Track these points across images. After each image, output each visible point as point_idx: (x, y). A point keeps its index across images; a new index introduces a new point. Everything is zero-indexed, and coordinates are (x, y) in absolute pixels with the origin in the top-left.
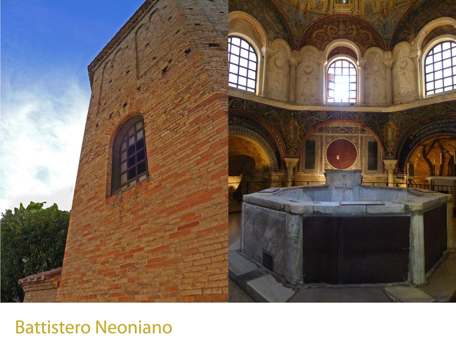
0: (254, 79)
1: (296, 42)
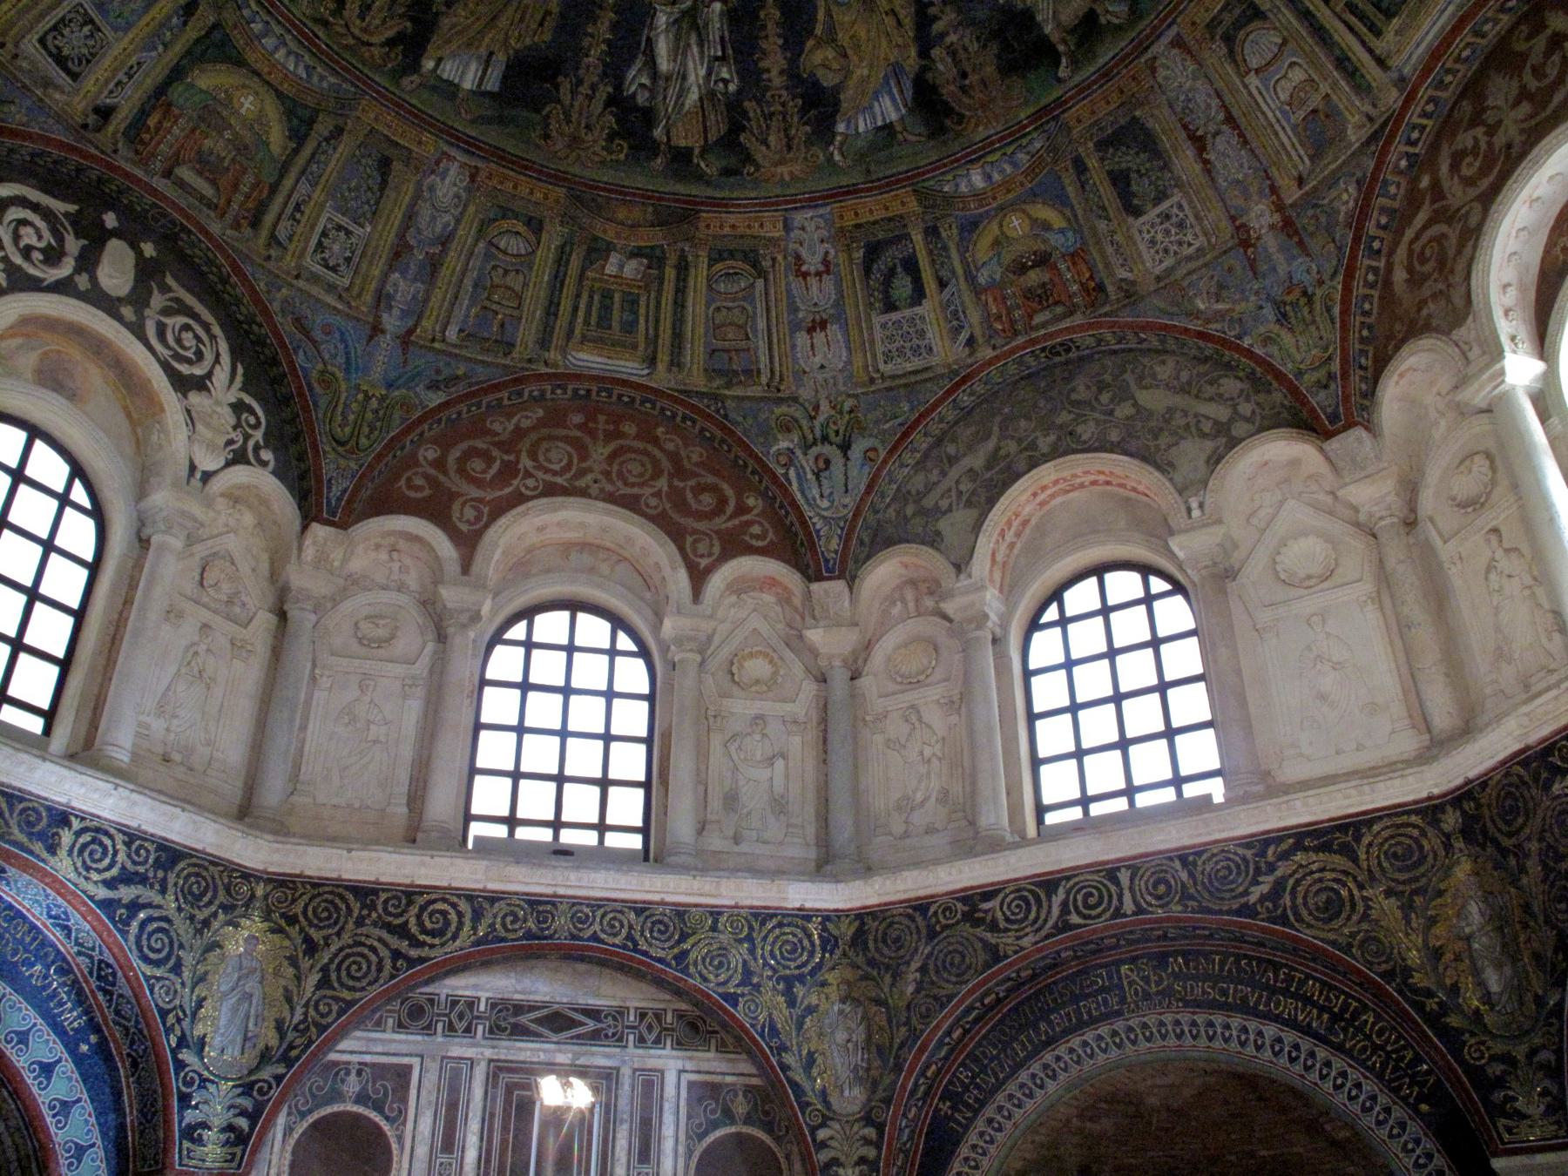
1: (1322, 394)
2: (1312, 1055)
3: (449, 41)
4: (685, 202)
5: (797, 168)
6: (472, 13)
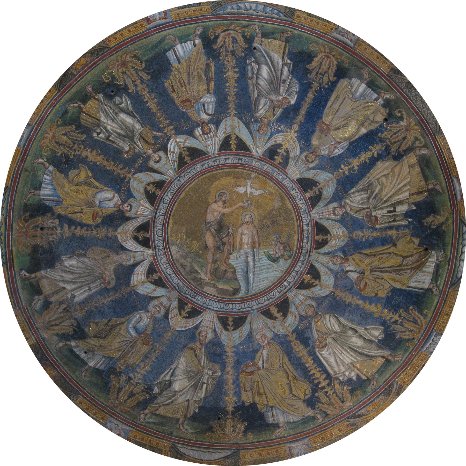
3: (197, 53)
4: (67, 88)
5: (47, 141)
6: (197, 69)
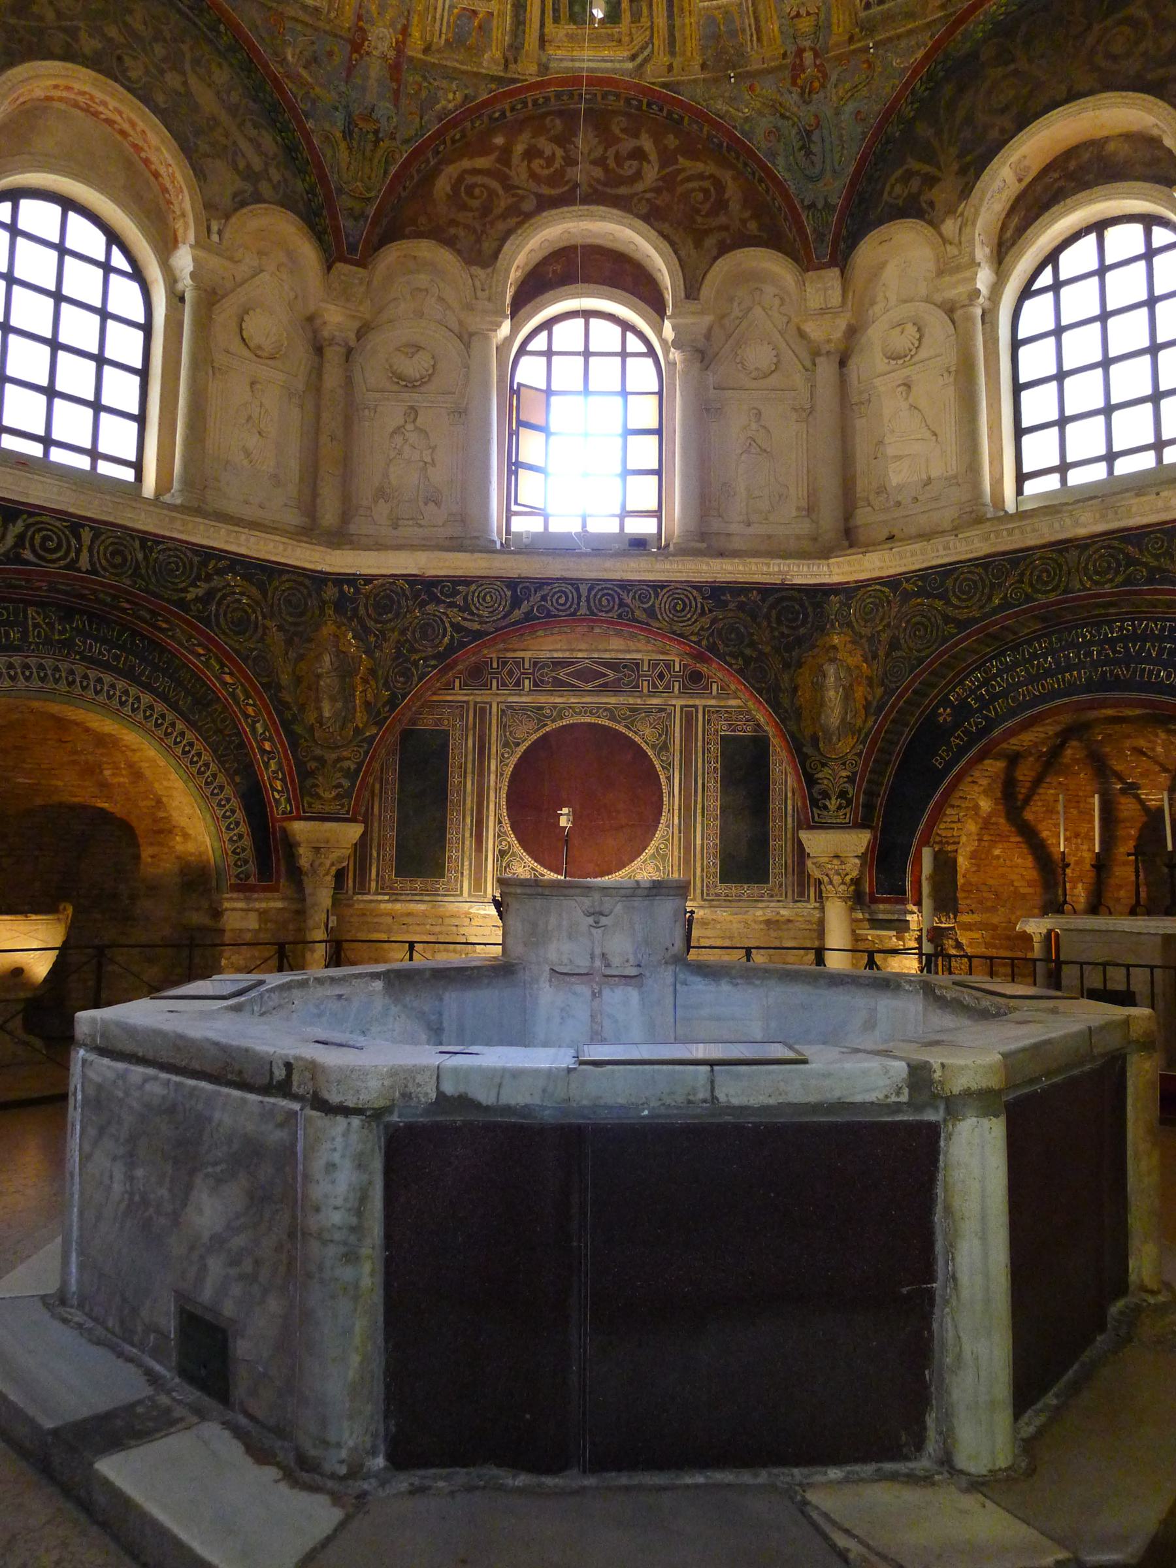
0: (135, 410)
1: (350, 223)
2: (173, 725)
